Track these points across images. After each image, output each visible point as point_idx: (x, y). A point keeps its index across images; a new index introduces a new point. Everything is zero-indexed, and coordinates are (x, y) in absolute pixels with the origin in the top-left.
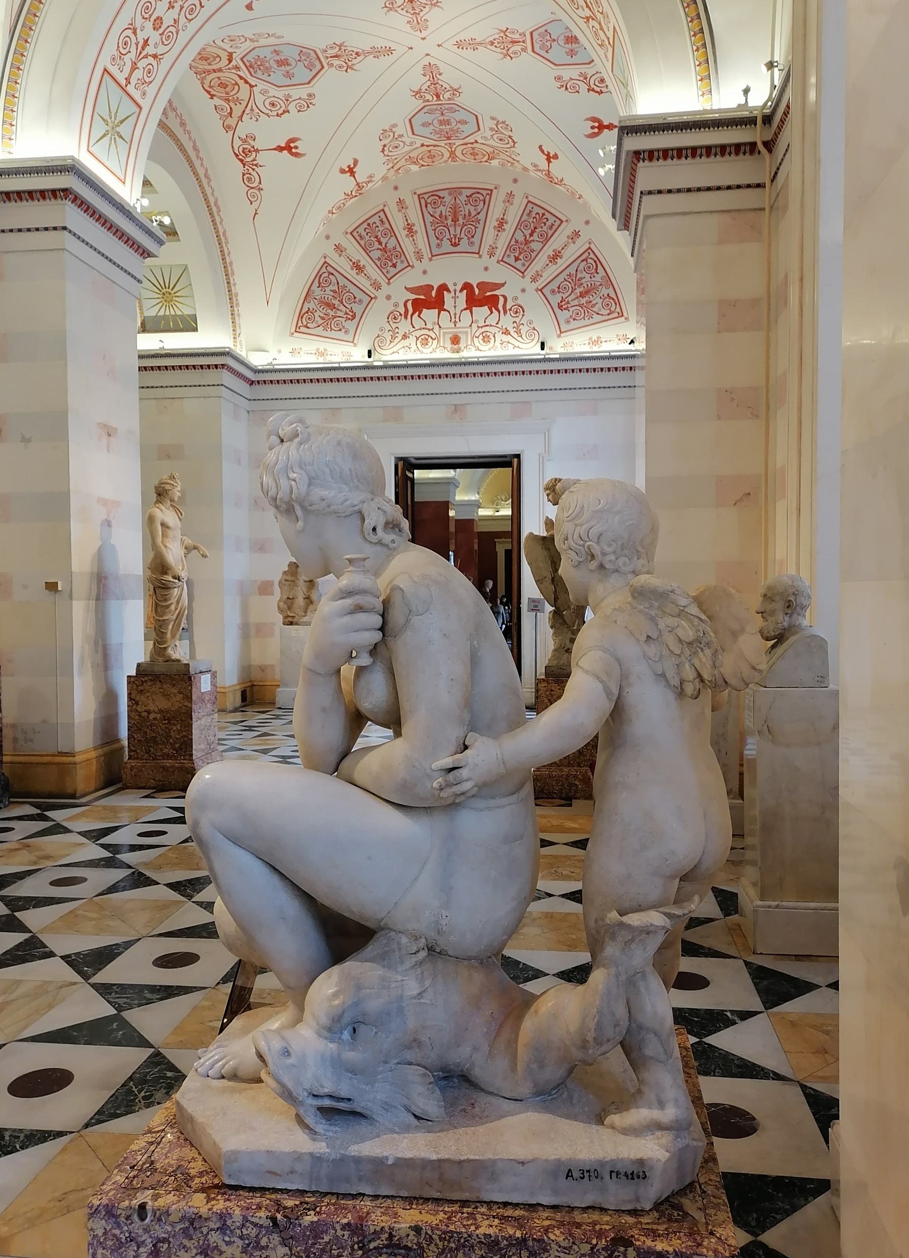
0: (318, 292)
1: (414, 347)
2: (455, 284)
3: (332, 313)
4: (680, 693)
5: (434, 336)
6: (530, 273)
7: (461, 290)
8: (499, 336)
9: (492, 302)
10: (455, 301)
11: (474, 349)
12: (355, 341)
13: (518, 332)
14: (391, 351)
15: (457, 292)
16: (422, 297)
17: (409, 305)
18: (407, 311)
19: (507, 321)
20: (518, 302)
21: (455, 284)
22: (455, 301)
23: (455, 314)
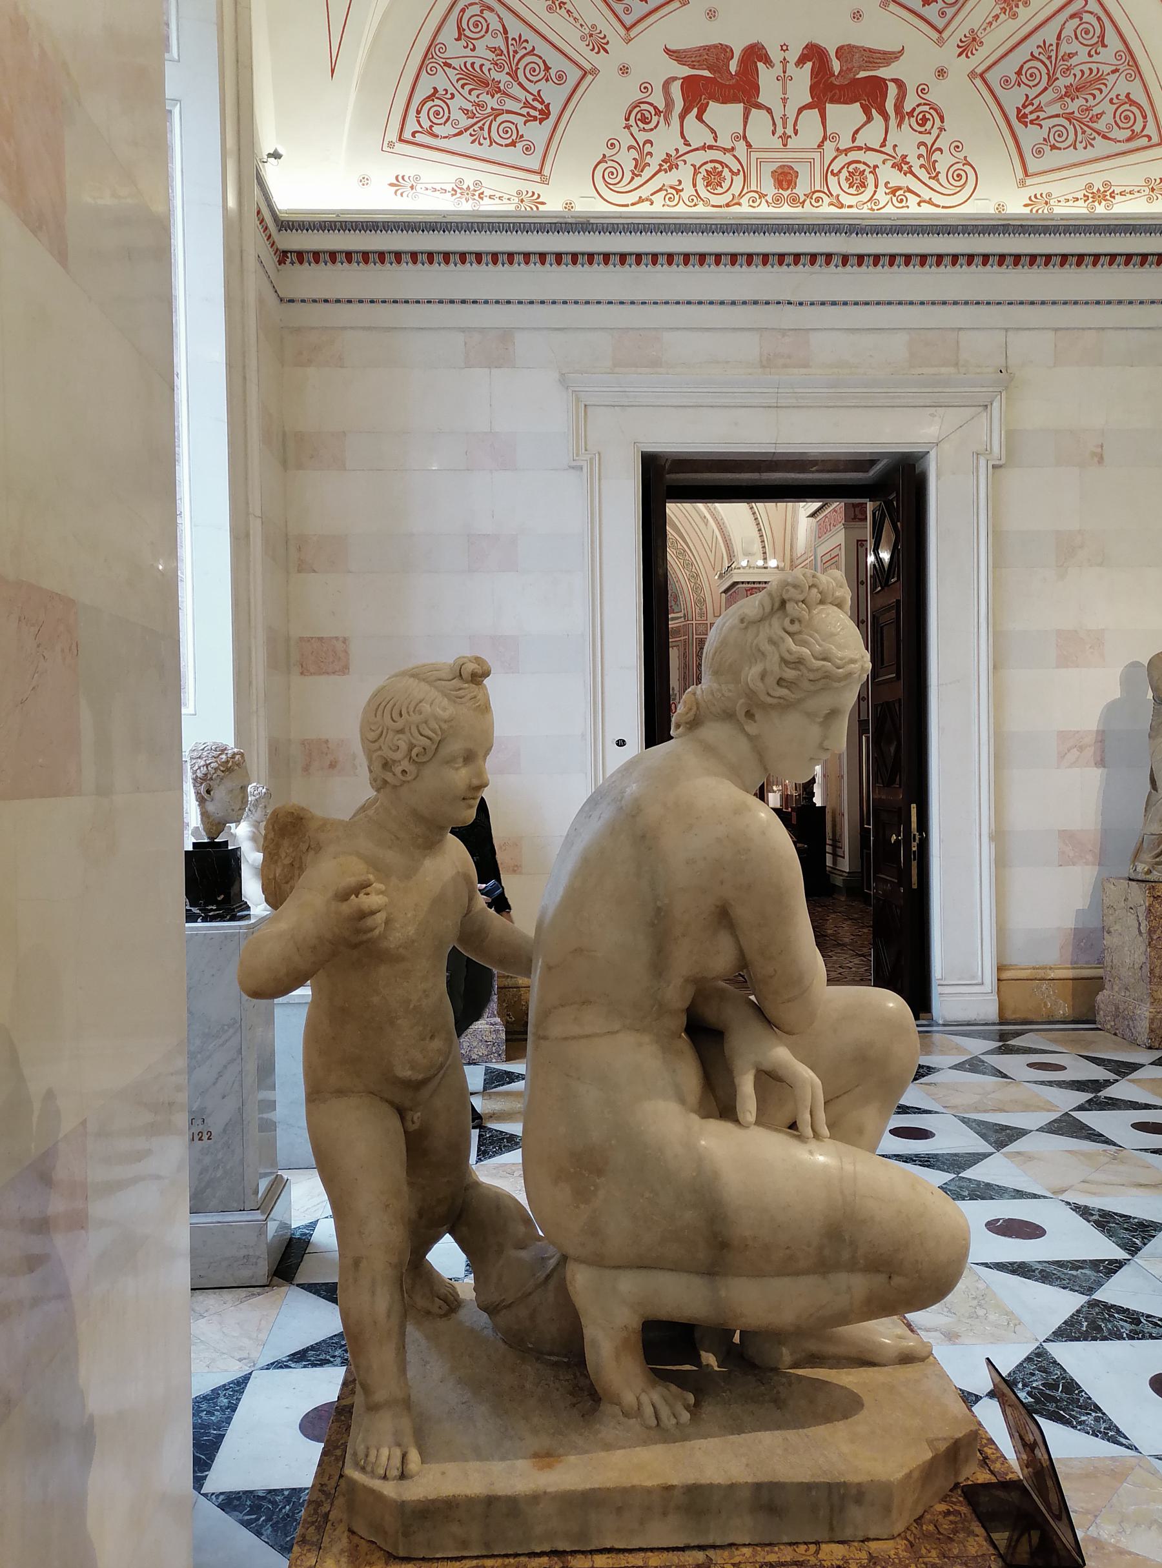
0: (455, 50)
1: (688, 191)
3: (492, 103)
5: (735, 166)
6: (959, 30)
7: (801, 61)
9: (870, 94)
10: (785, 87)
12: (546, 172)
13: (931, 167)
14: (633, 197)
15: (791, 67)
16: (706, 73)
17: (676, 90)
18: (669, 103)
19: (906, 140)
21: (784, 48)
22: (785, 87)
23: (784, 118)
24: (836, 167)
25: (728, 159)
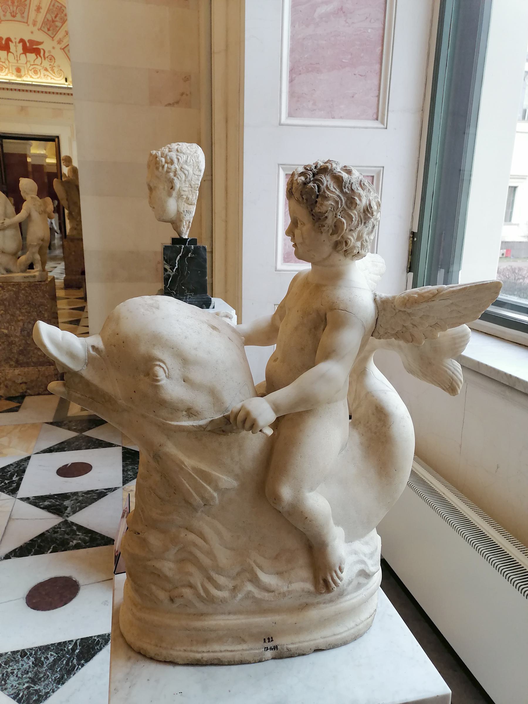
2: (15, 39)
4: (40, 214)
5: (6, 66)
7: (19, 42)
8: (43, 71)
9: (37, 52)
10: (16, 48)
11: (29, 76)
15: (17, 43)
19: (46, 63)
20: (52, 54)
21: (15, 39)
23: (17, 56)
24: (30, 68)
25: (4, 64)
